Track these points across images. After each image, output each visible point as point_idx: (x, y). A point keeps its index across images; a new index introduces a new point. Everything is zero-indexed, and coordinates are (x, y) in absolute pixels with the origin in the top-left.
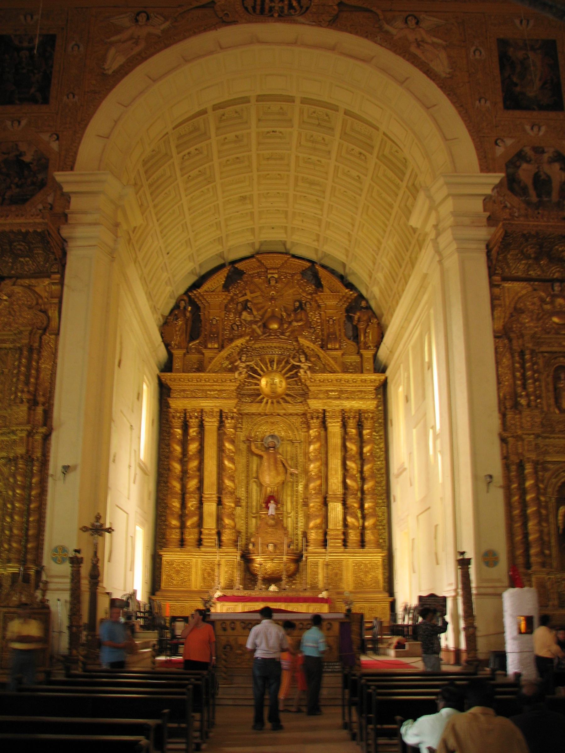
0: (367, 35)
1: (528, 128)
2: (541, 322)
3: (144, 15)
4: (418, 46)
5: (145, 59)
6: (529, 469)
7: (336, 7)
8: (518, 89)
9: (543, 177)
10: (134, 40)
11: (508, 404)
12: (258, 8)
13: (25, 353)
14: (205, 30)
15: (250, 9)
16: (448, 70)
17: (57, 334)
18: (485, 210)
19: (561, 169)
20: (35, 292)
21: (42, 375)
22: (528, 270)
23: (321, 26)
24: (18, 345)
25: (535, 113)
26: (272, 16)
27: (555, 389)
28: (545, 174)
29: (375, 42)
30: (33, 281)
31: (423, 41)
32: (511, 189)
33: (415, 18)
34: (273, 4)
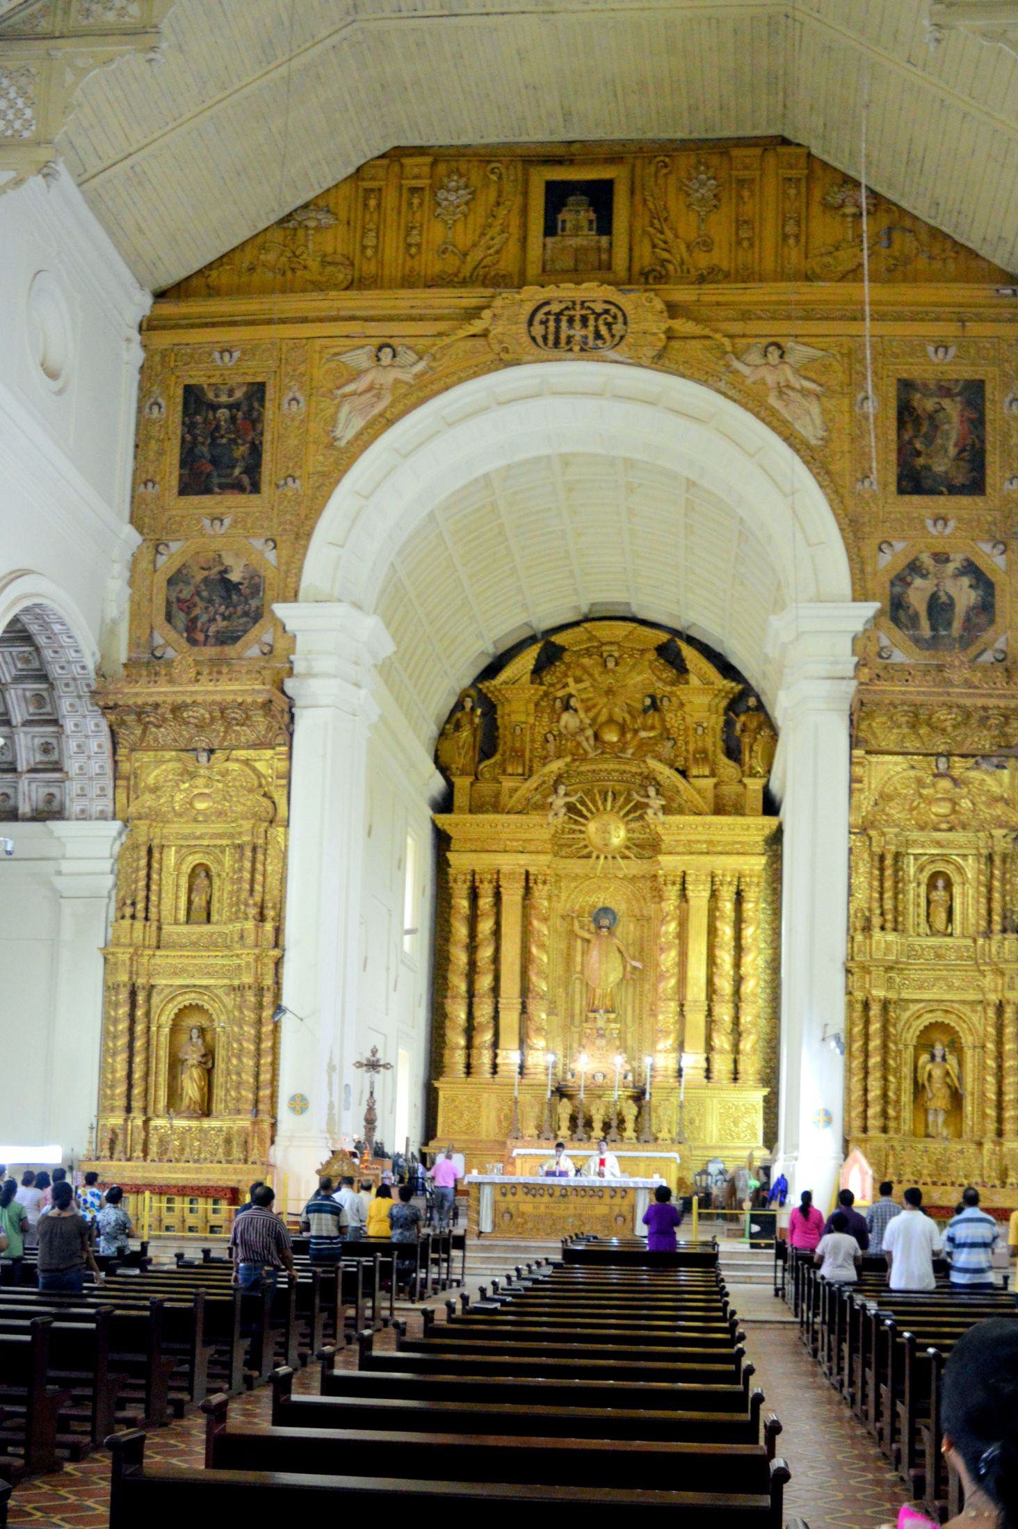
0: (705, 378)
1: (929, 523)
2: (915, 813)
3: (388, 350)
4: (781, 393)
5: (390, 423)
6: (875, 1010)
7: (663, 336)
8: (921, 461)
9: (944, 599)
10: (375, 392)
11: (859, 924)
12: (551, 338)
13: (248, 854)
14: (476, 375)
15: (540, 340)
16: (821, 433)
17: (288, 826)
18: (854, 653)
19: (971, 586)
20: (254, 770)
21: (269, 880)
22: (902, 741)
23: (641, 366)
24: (238, 842)
25: (942, 499)
26: (571, 350)
27: (929, 902)
28: (947, 593)
29: (718, 391)
30: (251, 754)
31: (788, 386)
32: (895, 620)
33: (778, 346)
34: (572, 332)
